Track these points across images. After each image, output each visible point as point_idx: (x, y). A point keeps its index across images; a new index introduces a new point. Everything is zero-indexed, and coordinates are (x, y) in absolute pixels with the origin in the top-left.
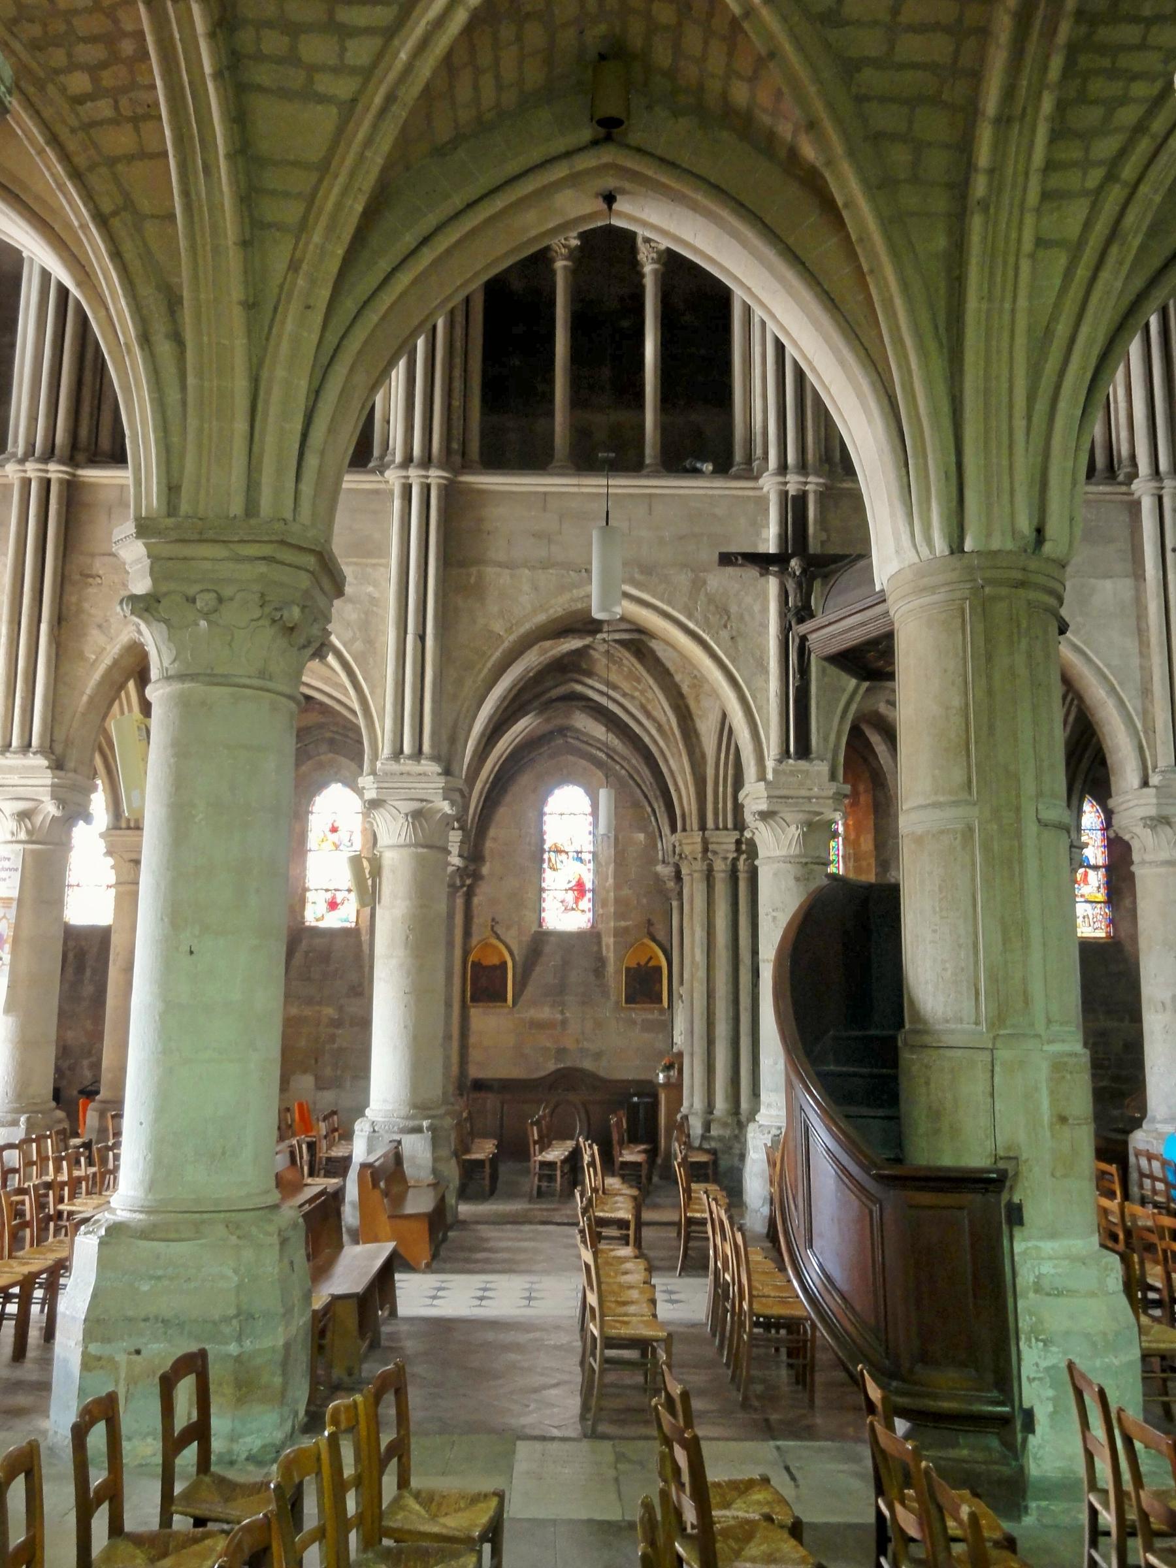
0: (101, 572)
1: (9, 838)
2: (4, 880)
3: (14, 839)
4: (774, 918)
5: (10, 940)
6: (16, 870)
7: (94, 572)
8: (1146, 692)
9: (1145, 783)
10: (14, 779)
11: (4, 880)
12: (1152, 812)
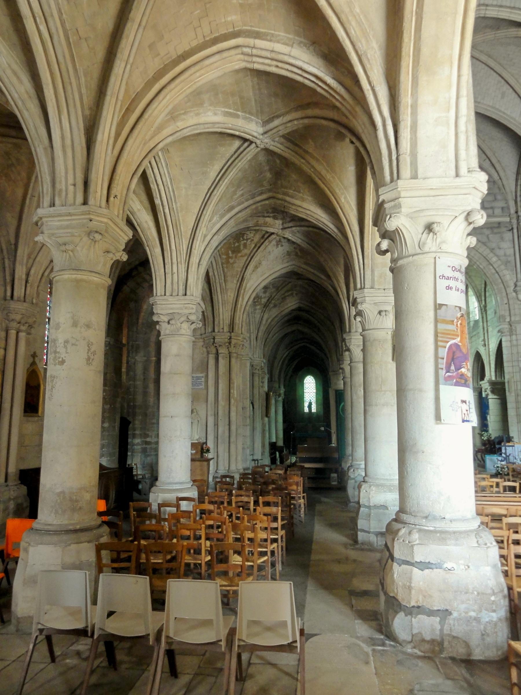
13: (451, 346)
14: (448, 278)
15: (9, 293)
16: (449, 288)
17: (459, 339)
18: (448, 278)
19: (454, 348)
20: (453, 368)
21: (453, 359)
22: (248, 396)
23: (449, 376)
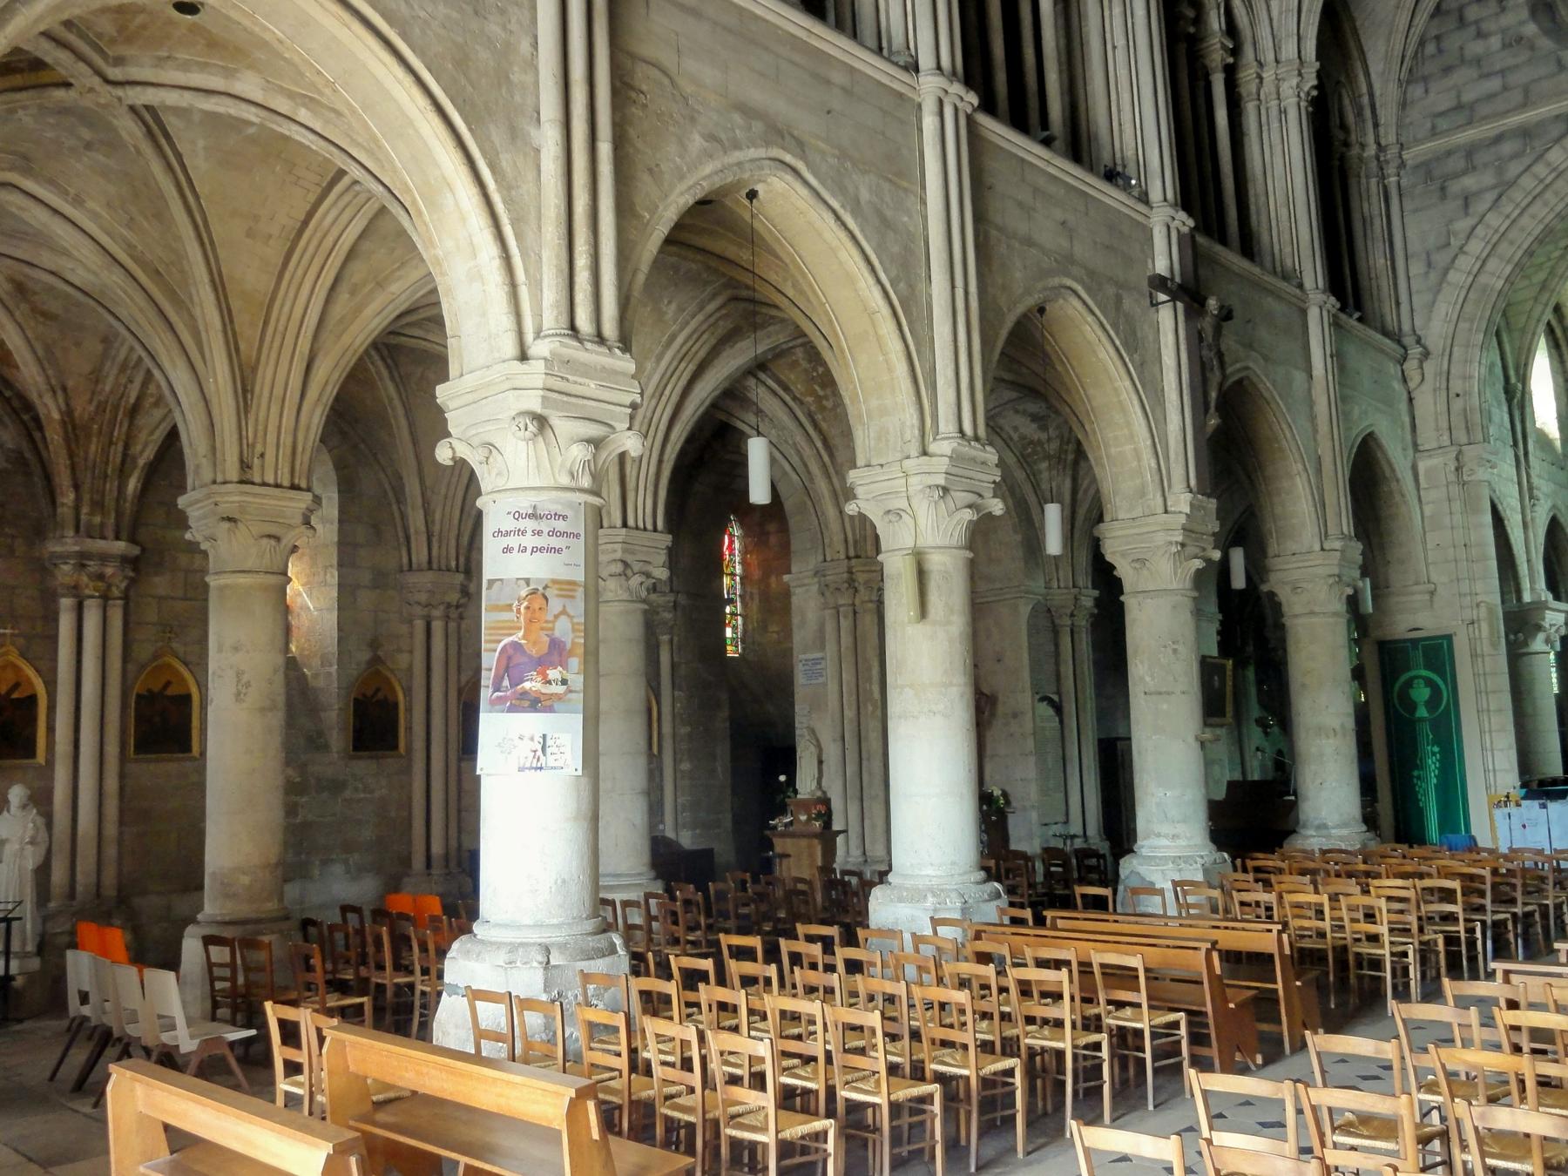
0: (644, 88)
1: (565, 480)
2: (559, 551)
3: (573, 484)
4: (1175, 651)
5: (580, 651)
6: (577, 536)
7: (637, 83)
8: (1319, 471)
9: (1322, 549)
10: (591, 387)
11: (559, 551)
12: (1336, 571)
13: (504, 649)
14: (508, 534)
15: (405, 560)
16: (508, 550)
17: (521, 634)
18: (508, 534)
19: (511, 651)
20: (506, 683)
21: (507, 669)
22: (1028, 685)
23: (499, 698)
